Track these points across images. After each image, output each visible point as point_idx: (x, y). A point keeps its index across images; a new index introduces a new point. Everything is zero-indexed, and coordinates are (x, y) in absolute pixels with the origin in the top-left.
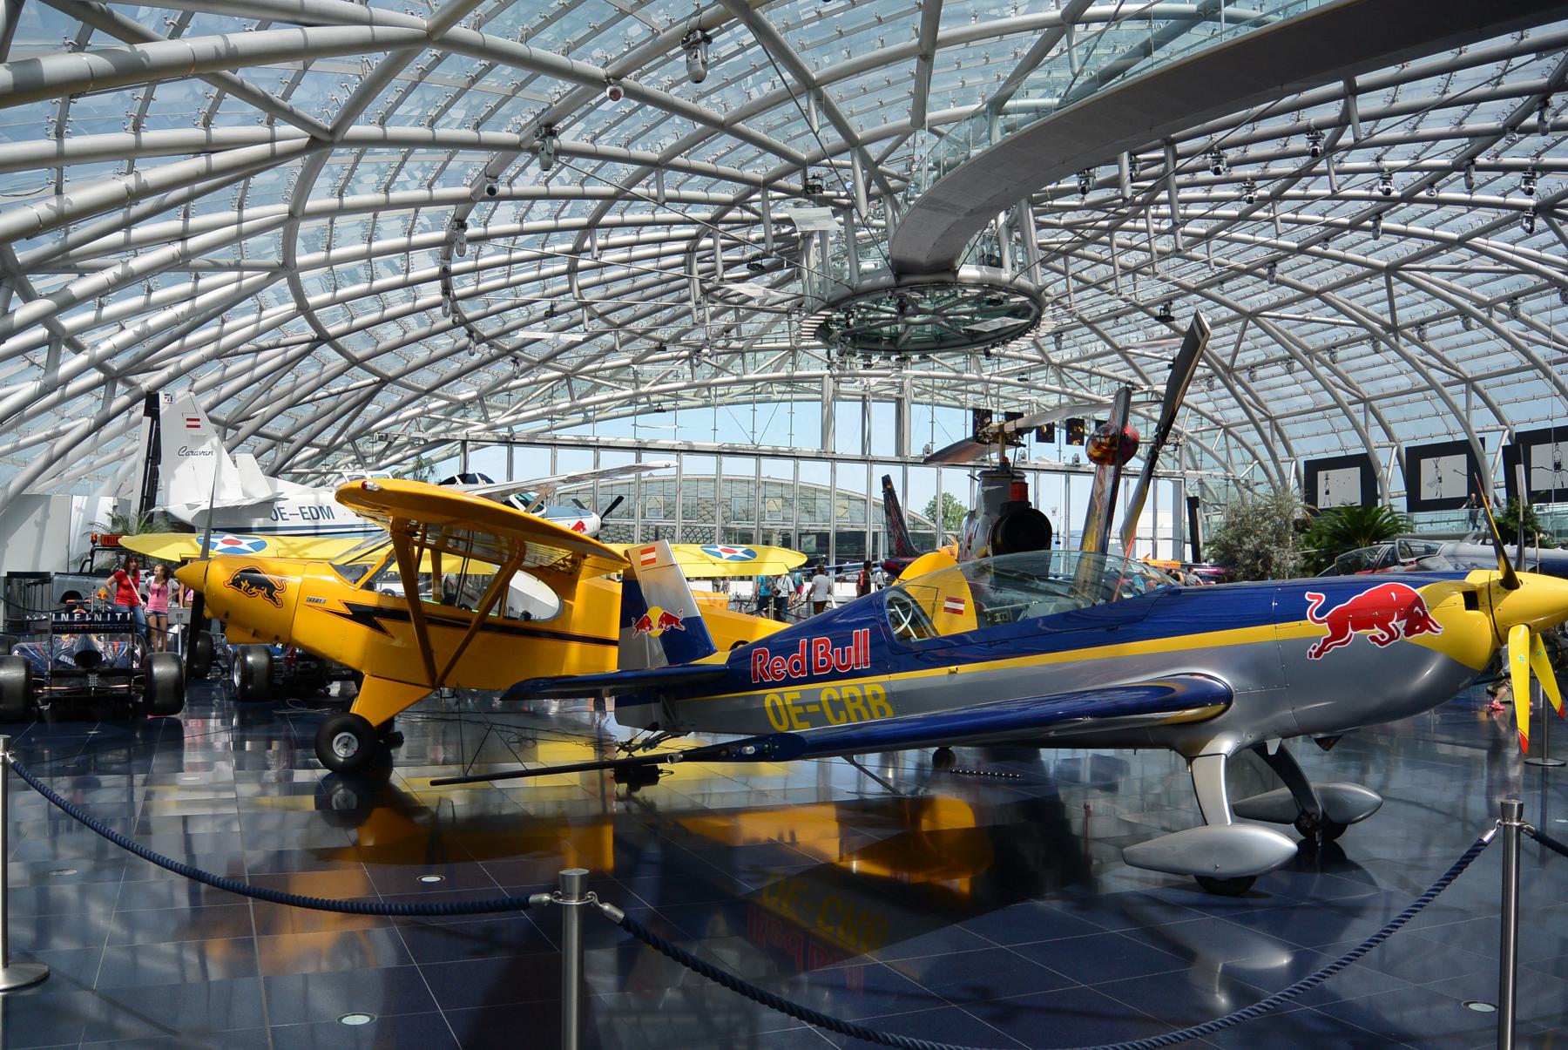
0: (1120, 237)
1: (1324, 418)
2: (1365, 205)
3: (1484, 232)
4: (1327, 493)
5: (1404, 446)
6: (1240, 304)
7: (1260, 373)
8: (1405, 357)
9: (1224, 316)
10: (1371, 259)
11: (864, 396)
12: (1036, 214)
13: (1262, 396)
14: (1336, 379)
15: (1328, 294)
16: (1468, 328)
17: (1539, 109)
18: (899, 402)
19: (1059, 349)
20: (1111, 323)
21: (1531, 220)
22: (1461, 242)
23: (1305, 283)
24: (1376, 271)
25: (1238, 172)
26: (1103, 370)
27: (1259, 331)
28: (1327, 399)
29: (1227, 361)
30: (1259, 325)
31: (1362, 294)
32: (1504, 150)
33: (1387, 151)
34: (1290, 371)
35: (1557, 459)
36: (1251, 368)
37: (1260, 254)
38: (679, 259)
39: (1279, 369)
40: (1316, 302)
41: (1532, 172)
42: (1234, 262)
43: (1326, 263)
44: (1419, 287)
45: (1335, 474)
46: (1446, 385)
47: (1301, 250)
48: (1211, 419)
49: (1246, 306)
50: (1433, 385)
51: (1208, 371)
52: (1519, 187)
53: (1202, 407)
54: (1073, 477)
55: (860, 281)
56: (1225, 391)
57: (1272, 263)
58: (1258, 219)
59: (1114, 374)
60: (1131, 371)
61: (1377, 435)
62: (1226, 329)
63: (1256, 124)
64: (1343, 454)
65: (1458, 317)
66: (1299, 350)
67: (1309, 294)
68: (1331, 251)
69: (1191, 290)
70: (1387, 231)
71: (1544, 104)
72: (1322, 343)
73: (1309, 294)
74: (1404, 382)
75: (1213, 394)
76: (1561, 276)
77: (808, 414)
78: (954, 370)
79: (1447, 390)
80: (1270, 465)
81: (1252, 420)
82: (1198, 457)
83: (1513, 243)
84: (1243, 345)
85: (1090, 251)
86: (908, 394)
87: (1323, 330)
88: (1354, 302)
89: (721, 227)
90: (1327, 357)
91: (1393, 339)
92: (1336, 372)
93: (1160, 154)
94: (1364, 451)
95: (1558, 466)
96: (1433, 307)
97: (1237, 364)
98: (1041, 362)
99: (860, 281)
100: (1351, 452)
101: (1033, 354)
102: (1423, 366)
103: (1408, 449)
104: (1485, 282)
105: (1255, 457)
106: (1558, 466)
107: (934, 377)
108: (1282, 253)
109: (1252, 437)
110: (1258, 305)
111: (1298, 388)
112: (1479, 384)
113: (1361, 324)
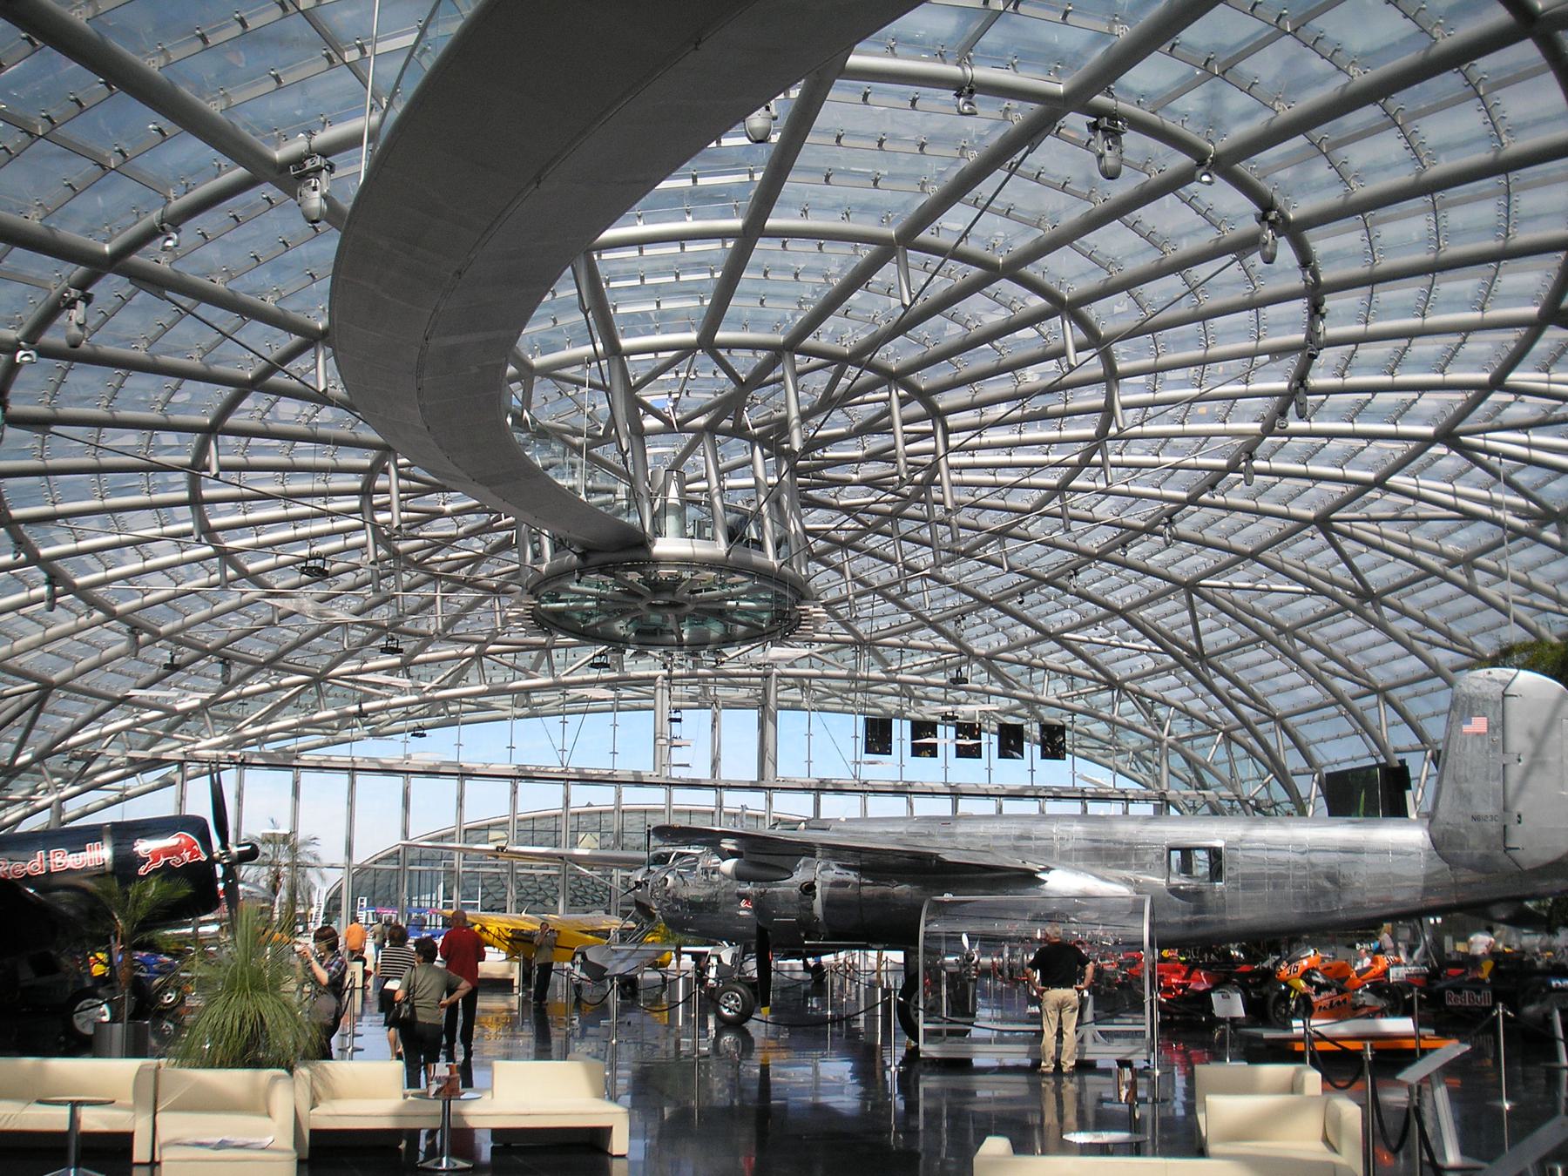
0: (905, 526)
85: (873, 541)
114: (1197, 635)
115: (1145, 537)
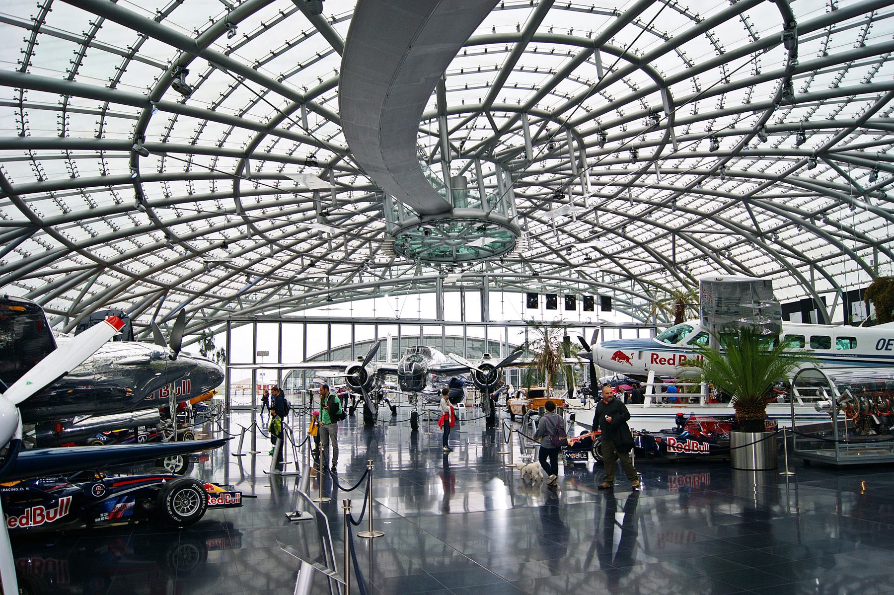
6: (668, 225)
23: (701, 210)
24: (738, 199)
49: (672, 225)
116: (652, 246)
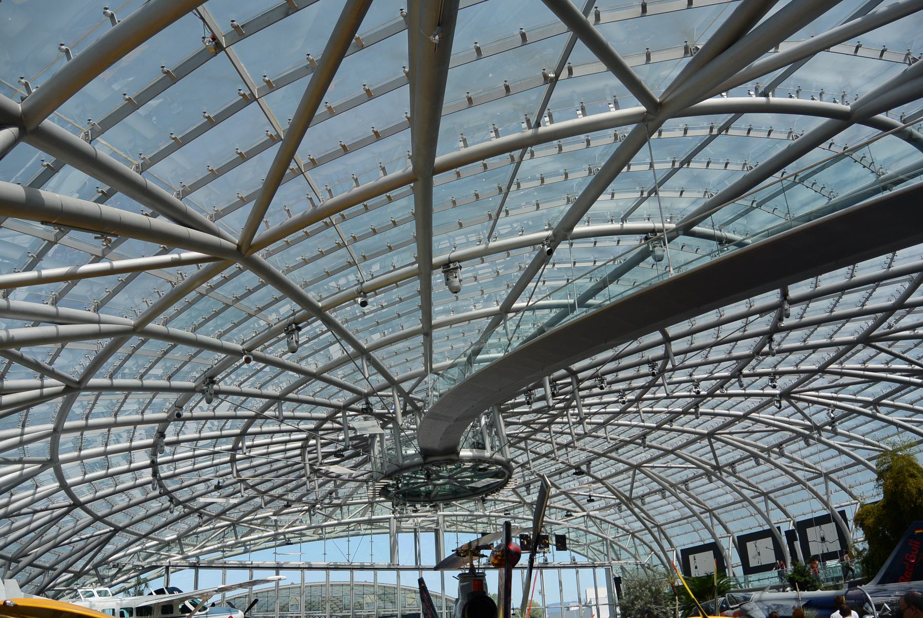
0: (555, 428)
1: (688, 523)
2: (689, 400)
3: (757, 410)
4: (696, 568)
5: (736, 535)
6: (630, 461)
7: (647, 500)
8: (727, 484)
9: (622, 468)
10: (698, 430)
11: (415, 529)
12: (504, 418)
13: (651, 513)
14: (691, 500)
15: (678, 451)
16: (758, 464)
17: (769, 342)
18: (437, 532)
19: (529, 494)
20: (557, 477)
21: (779, 402)
22: (745, 417)
23: (664, 446)
24: (702, 436)
25: (615, 387)
26: (556, 505)
27: (642, 475)
28: (688, 512)
29: (627, 494)
30: (642, 472)
31: (697, 450)
32: (757, 365)
33: (694, 371)
34: (664, 497)
35: (822, 535)
36: (642, 497)
37: (637, 432)
38: (298, 452)
39: (658, 496)
40: (672, 456)
41: (774, 376)
42: (622, 437)
43: (673, 434)
44: (727, 443)
45: (699, 556)
46: (753, 498)
47: (658, 428)
48: (623, 529)
50: (745, 499)
51: (618, 501)
52: (768, 385)
53: (617, 522)
54: (544, 571)
55: (403, 461)
56: (629, 512)
57: (643, 437)
58: (629, 412)
59: (563, 507)
60: (573, 504)
61: (719, 531)
62: (624, 476)
63: (620, 360)
64: (702, 543)
65: (752, 458)
66: (667, 485)
67: (667, 452)
68: (675, 426)
69: (600, 455)
70: (702, 414)
71: (771, 340)
72: (680, 479)
73: (667, 452)
74: (730, 498)
75: (623, 514)
76: (802, 431)
77: (382, 542)
78: (469, 511)
79: (754, 501)
80: (661, 554)
81: (647, 528)
82: (618, 552)
83: (773, 415)
84: (635, 484)
85: (539, 436)
86: (441, 528)
87: (679, 472)
88: (693, 455)
89: (321, 433)
90: (683, 487)
91: (719, 474)
92: (690, 496)
93: (569, 380)
94: (713, 541)
95: (823, 539)
96: (738, 454)
97: (633, 496)
98: (520, 503)
99: (403, 461)
100: (707, 542)
101: (514, 498)
102: (738, 488)
103: (738, 537)
104: (763, 438)
105: (652, 550)
106: (823, 539)
107: (457, 516)
108: (648, 430)
109: (648, 538)
110: (640, 461)
111: (670, 507)
112: (771, 495)
113: (699, 467)
114: (715, 457)
115: (682, 416)
116: (609, 482)
